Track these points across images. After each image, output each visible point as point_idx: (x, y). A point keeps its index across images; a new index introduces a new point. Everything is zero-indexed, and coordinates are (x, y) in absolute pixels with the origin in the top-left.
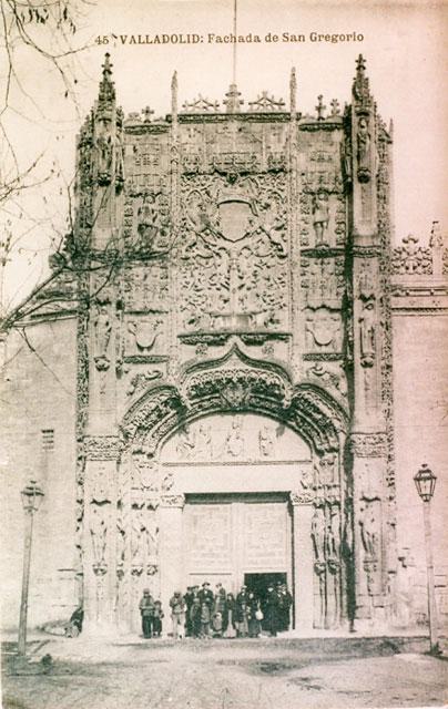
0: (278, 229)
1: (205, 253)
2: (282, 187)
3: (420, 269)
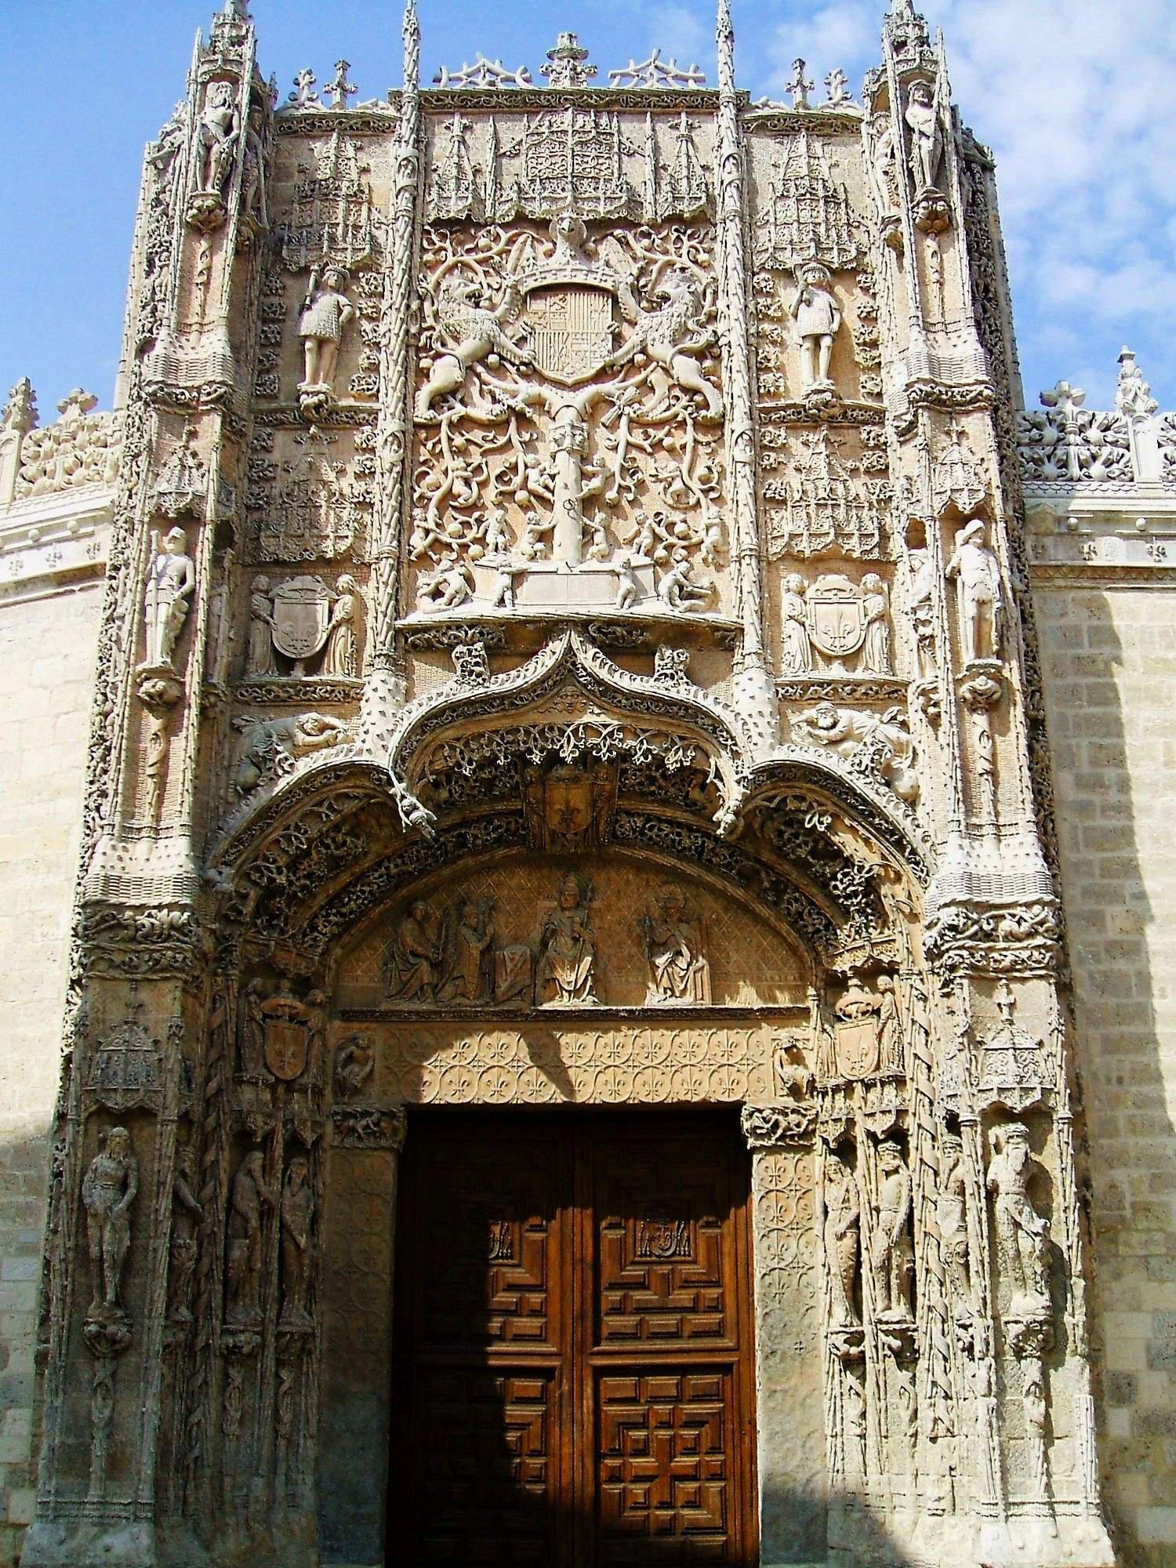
0: (700, 355)
1: (482, 409)
2: (702, 257)
3: (1097, 469)
